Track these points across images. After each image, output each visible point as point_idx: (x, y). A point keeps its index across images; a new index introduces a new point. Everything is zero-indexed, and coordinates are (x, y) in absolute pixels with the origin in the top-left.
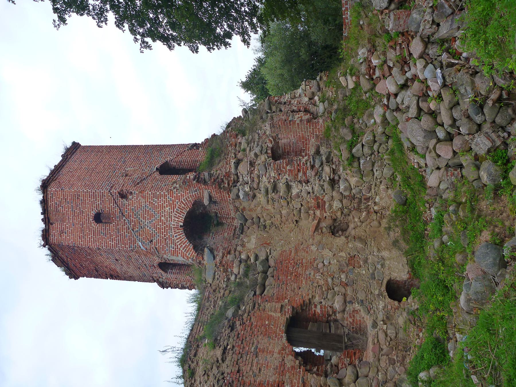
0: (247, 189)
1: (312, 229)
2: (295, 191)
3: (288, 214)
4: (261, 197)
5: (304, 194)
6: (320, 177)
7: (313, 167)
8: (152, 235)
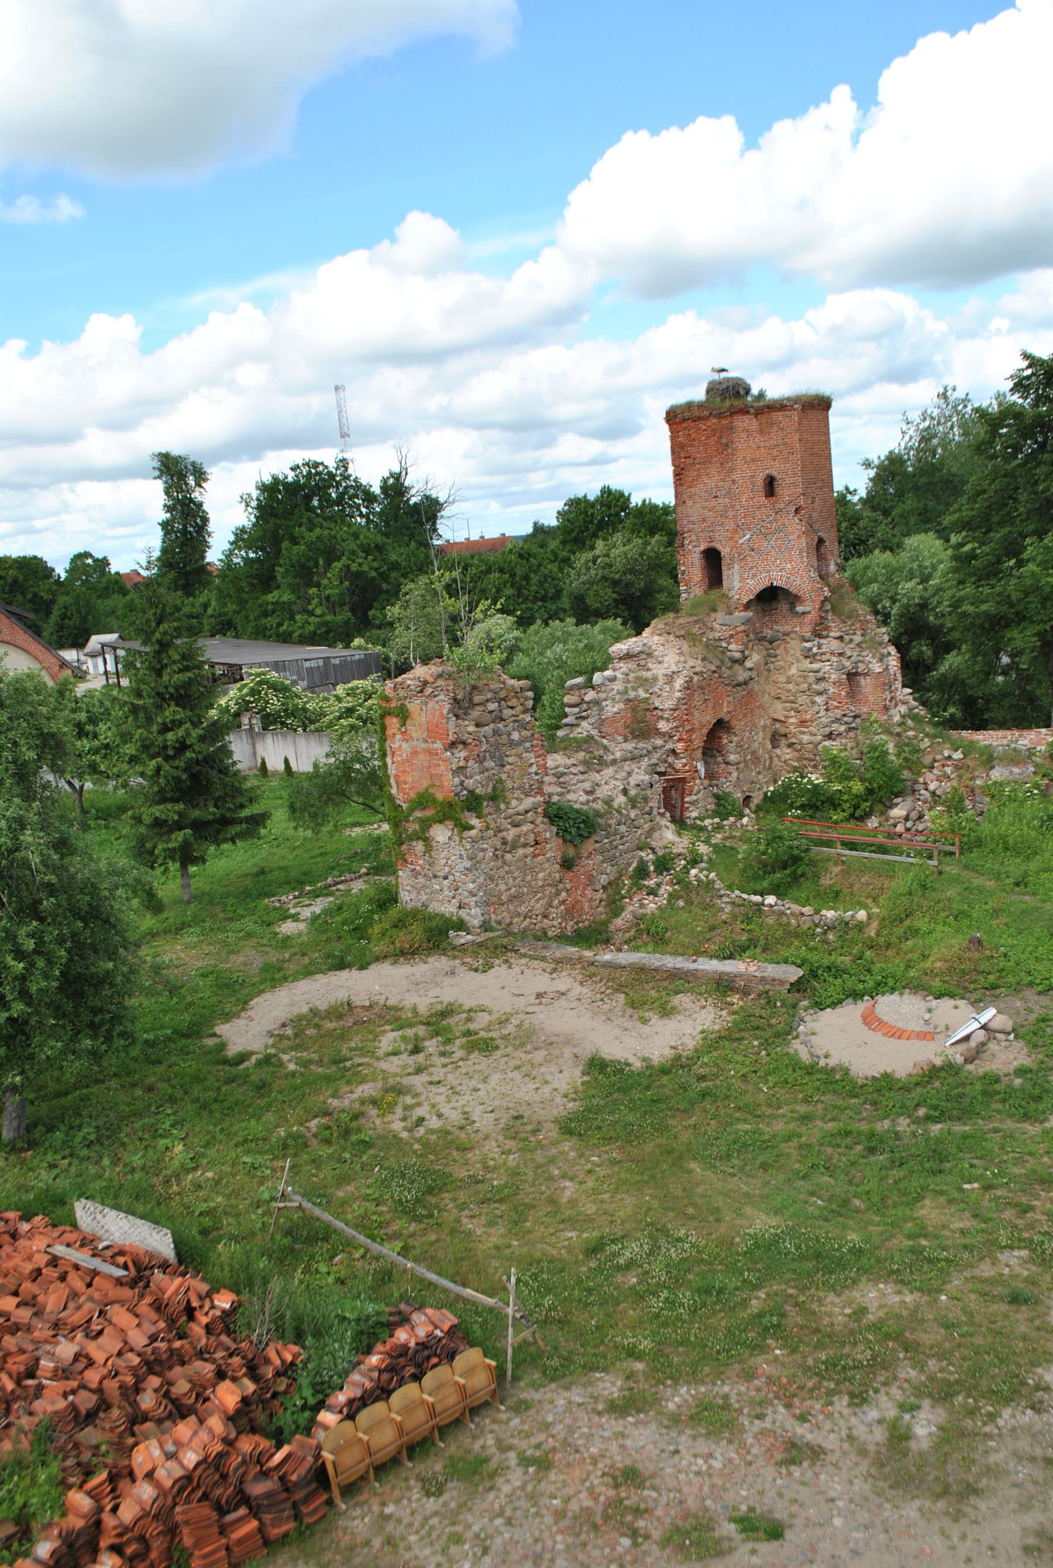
0: (815, 650)
1: (776, 716)
2: (818, 699)
3: (789, 691)
4: (806, 664)
5: (816, 708)
6: (833, 722)
7: (845, 715)
8: (759, 549)
